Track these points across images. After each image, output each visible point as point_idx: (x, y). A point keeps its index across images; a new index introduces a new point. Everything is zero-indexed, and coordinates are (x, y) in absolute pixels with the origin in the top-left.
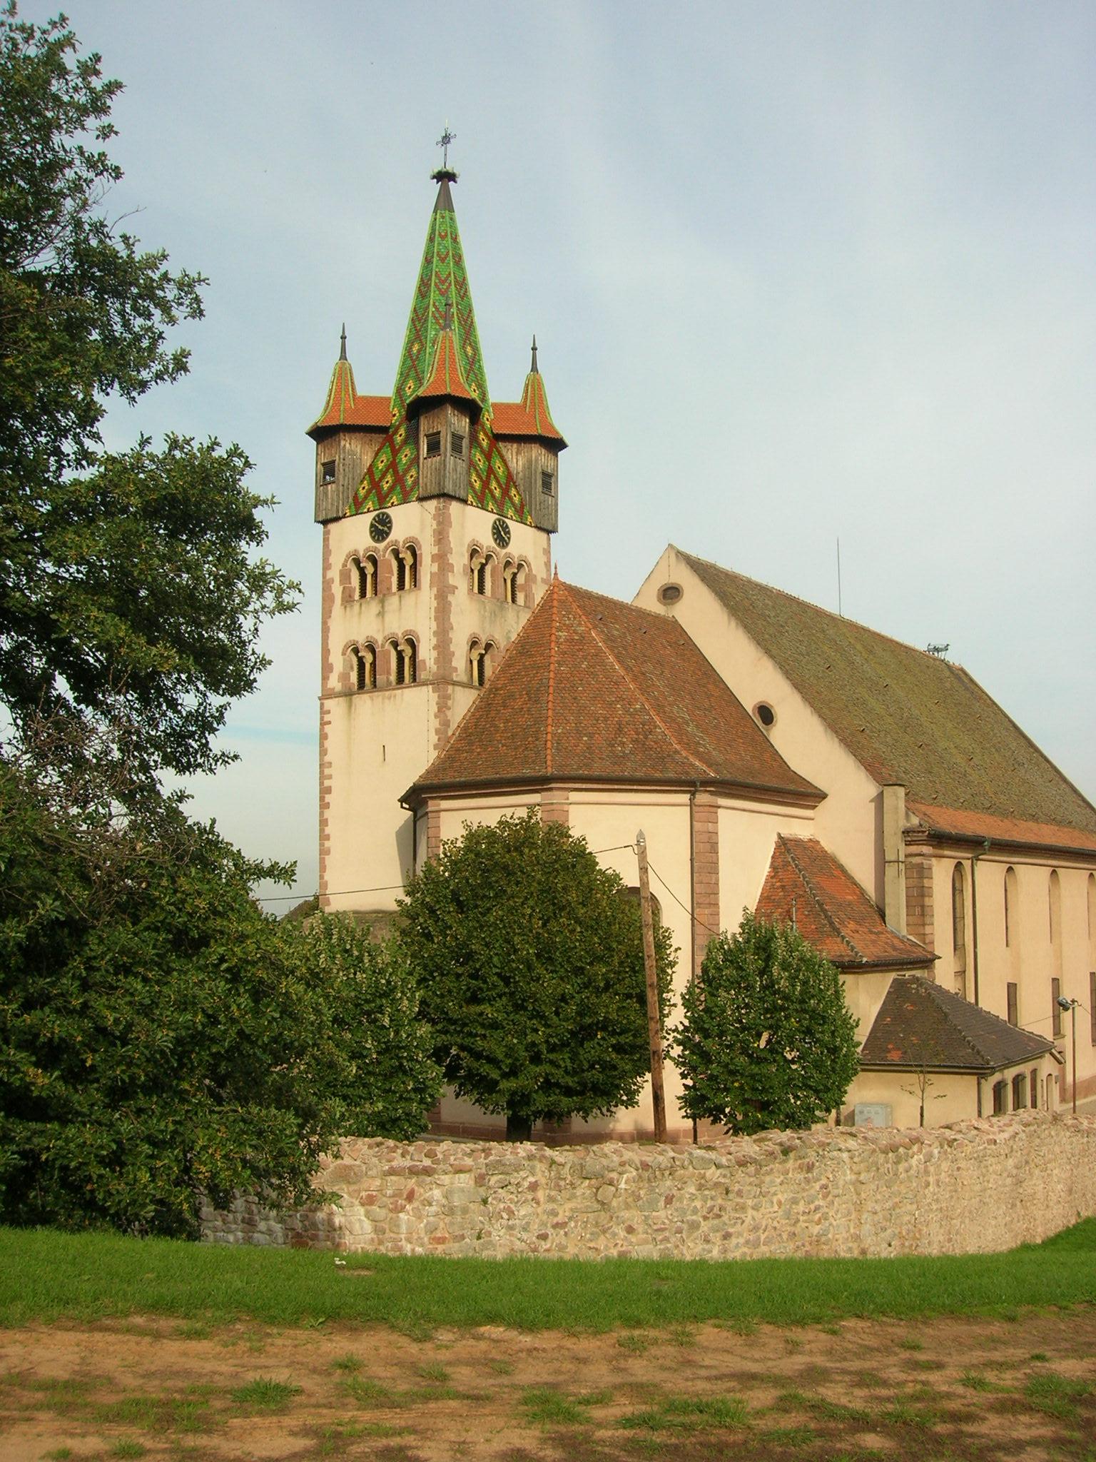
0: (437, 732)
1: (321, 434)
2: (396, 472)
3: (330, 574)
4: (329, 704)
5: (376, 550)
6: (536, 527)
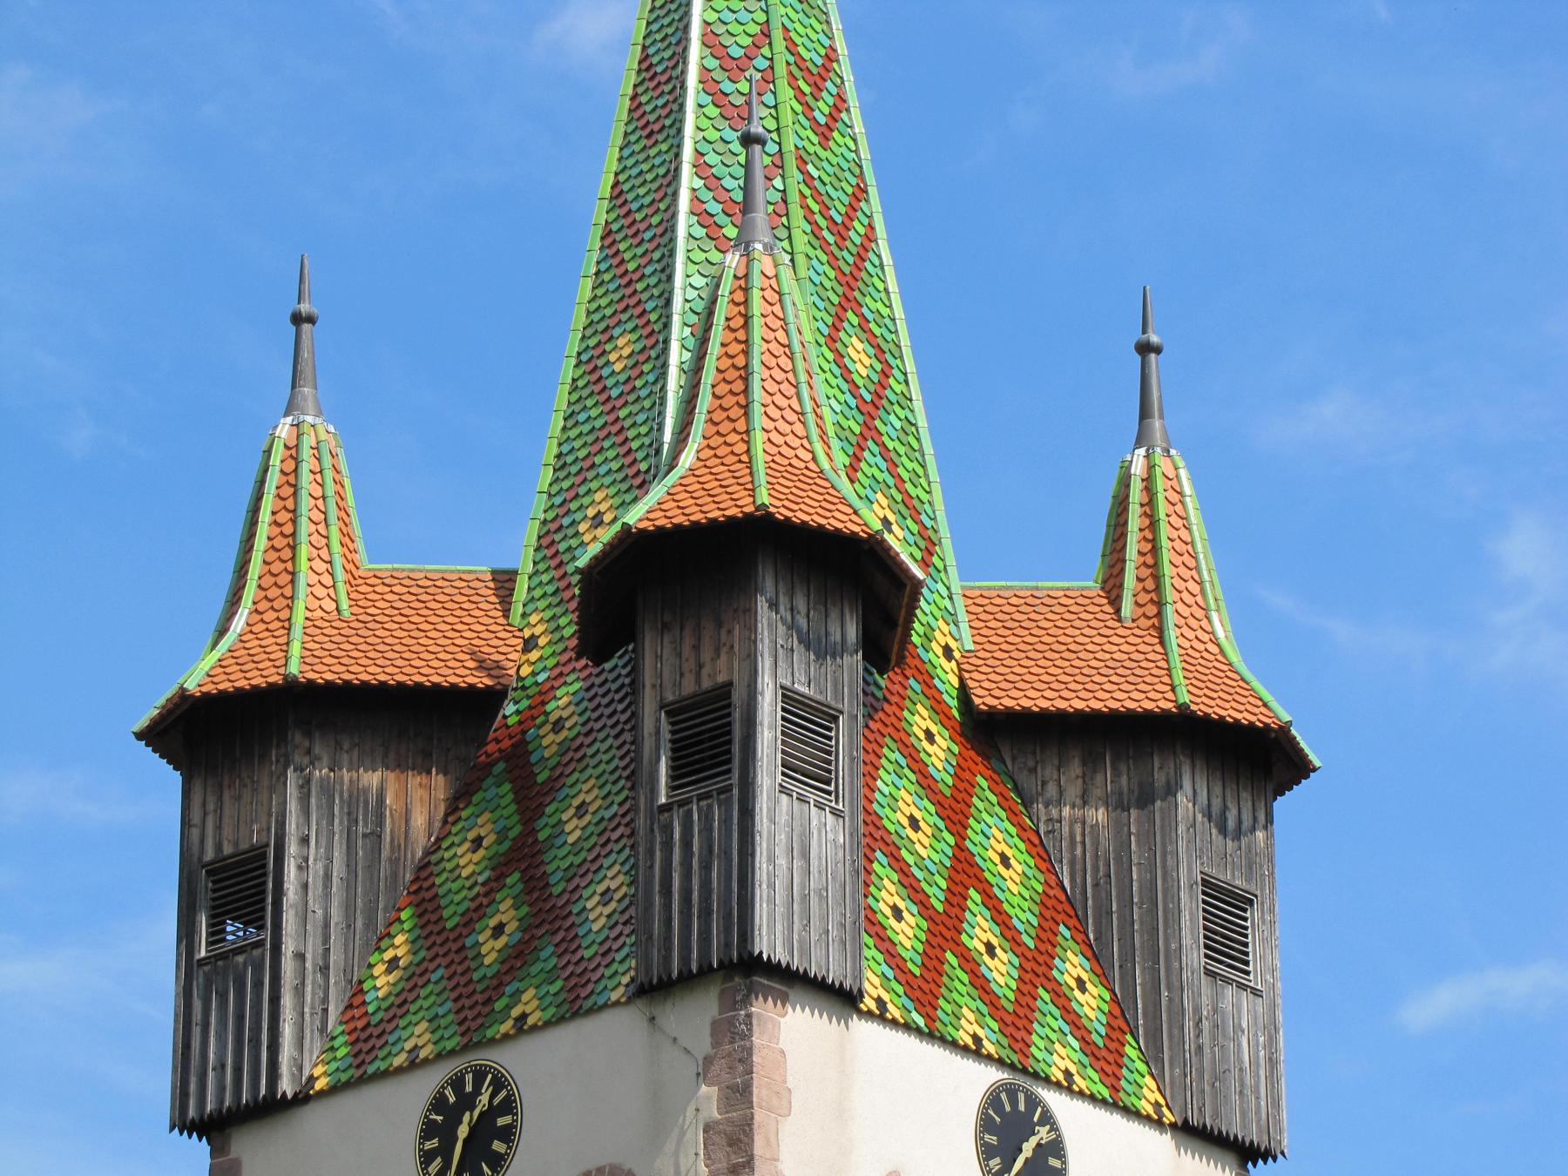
1: (212, 736)
2: (536, 885)
6: (1194, 1133)
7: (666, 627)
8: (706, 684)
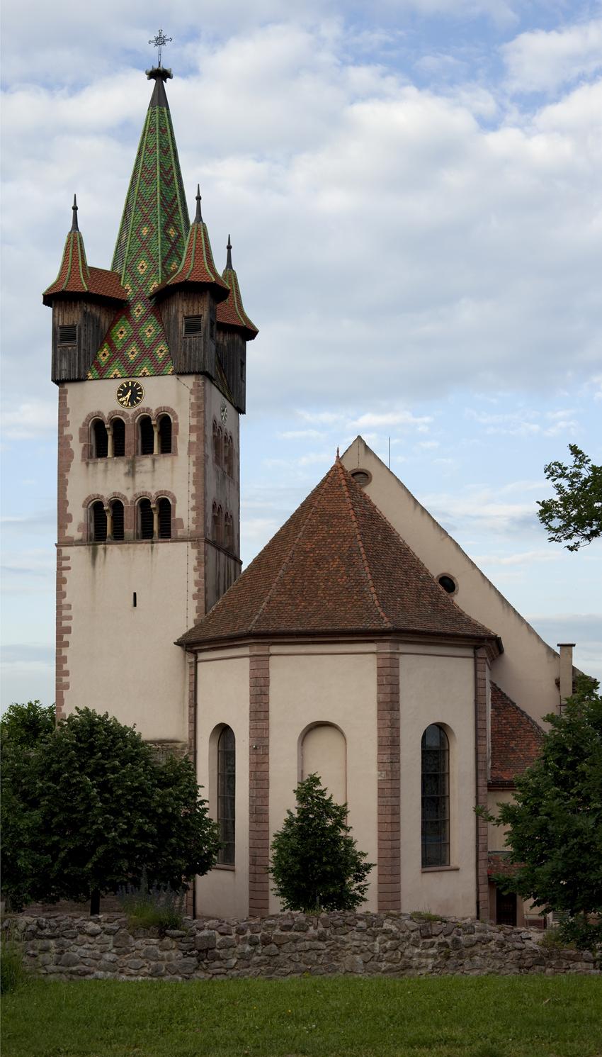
0: (196, 583)
3: (67, 431)
4: (67, 551)
5: (123, 414)
7: (185, 300)
8: (195, 314)
